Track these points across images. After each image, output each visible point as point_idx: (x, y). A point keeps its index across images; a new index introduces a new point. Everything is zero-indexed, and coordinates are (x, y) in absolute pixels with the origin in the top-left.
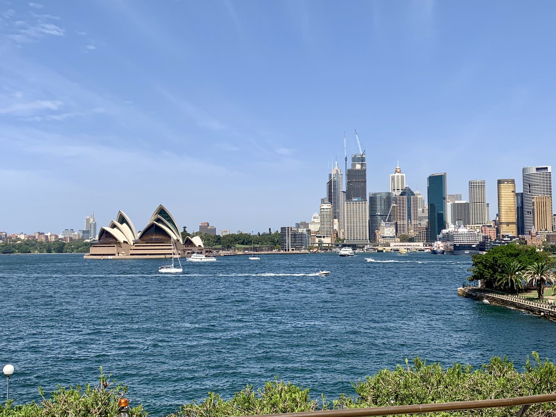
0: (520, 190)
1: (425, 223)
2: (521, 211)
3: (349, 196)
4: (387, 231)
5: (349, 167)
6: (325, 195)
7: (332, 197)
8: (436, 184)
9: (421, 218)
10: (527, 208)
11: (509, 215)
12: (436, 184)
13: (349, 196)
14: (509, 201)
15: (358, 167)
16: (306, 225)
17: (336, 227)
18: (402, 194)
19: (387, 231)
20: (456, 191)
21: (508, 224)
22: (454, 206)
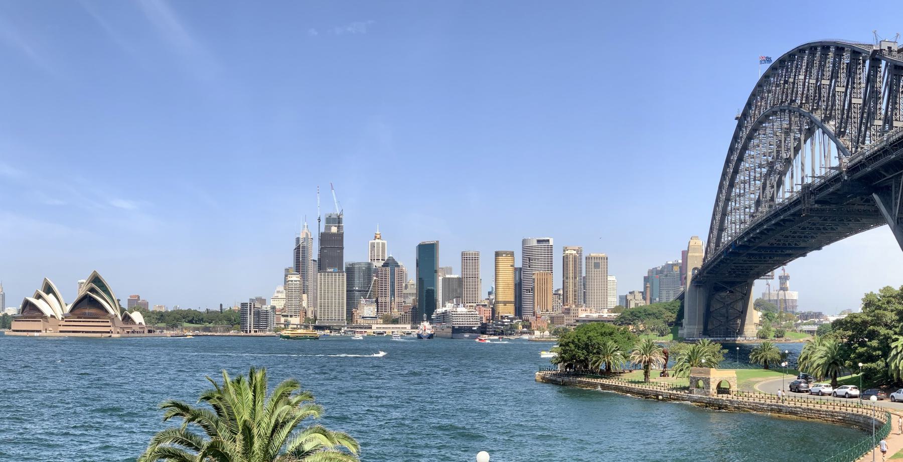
0: (519, 264)
1: (410, 301)
2: (519, 287)
3: (321, 266)
4: (367, 310)
5: (323, 230)
6: (291, 263)
7: (300, 265)
8: (427, 254)
9: (406, 296)
10: (526, 285)
11: (507, 293)
12: (427, 254)
13: (321, 266)
14: (507, 277)
15: (334, 230)
16: (263, 301)
17: (305, 304)
18: (386, 265)
19: (367, 310)
20: (449, 264)
21: (505, 303)
22: (444, 280)
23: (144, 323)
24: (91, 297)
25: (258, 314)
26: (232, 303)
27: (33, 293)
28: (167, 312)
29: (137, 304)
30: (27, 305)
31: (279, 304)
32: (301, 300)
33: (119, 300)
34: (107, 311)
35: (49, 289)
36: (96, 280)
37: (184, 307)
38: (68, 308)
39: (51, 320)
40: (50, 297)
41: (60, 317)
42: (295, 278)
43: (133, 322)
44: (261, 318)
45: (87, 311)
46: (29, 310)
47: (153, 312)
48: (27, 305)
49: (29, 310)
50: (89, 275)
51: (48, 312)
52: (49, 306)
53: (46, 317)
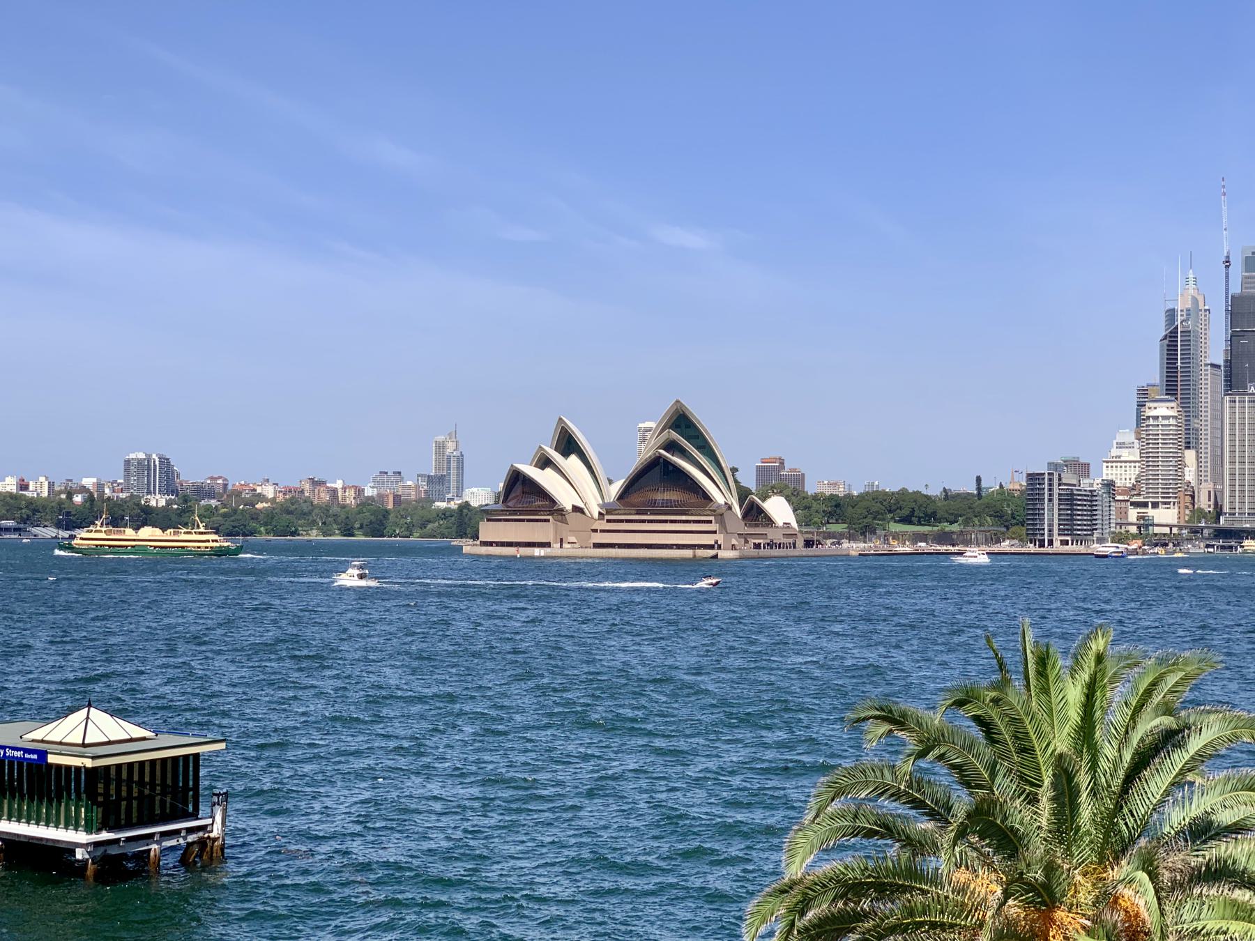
17: (1190, 475)
23: (794, 525)
24: (667, 463)
25: (1069, 499)
26: (1005, 475)
27: (532, 453)
28: (849, 496)
29: (777, 479)
31: (1124, 476)
32: (1181, 464)
33: (734, 470)
34: (707, 497)
35: (568, 445)
36: (681, 422)
37: (890, 485)
38: (614, 490)
39: (573, 518)
40: (572, 464)
41: (595, 511)
42: (1164, 410)
43: (769, 522)
44: (1080, 511)
45: (660, 496)
46: (522, 495)
47: (816, 497)
48: (517, 481)
49: (522, 495)
51: (565, 497)
52: (570, 485)
53: (561, 512)
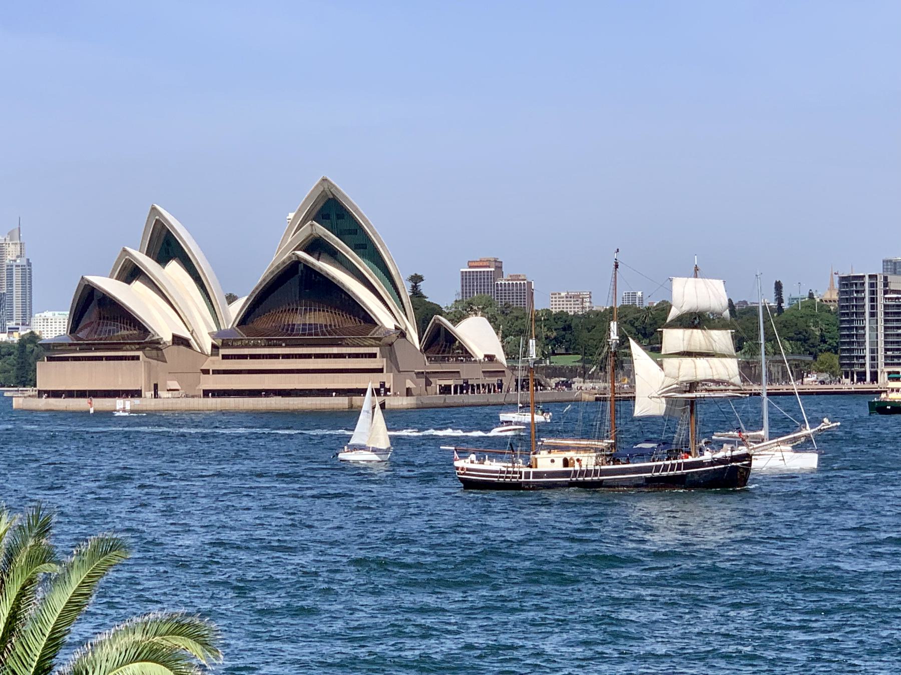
23: (501, 357)
24: (310, 271)
27: (112, 260)
30: (93, 307)
34: (368, 320)
35: (166, 247)
36: (330, 210)
38: (235, 310)
39: (172, 353)
40: (173, 273)
41: (207, 344)
43: (467, 354)
45: (298, 320)
46: (100, 319)
48: (93, 307)
49: (100, 319)
50: (303, 194)
51: (163, 324)
53: (153, 346)
